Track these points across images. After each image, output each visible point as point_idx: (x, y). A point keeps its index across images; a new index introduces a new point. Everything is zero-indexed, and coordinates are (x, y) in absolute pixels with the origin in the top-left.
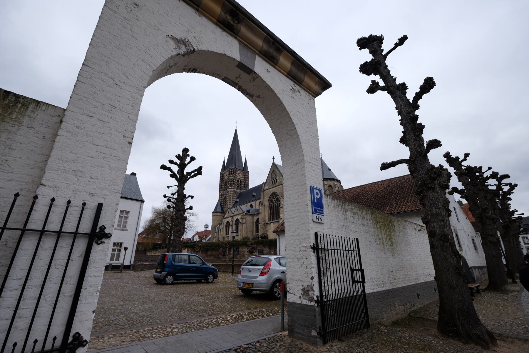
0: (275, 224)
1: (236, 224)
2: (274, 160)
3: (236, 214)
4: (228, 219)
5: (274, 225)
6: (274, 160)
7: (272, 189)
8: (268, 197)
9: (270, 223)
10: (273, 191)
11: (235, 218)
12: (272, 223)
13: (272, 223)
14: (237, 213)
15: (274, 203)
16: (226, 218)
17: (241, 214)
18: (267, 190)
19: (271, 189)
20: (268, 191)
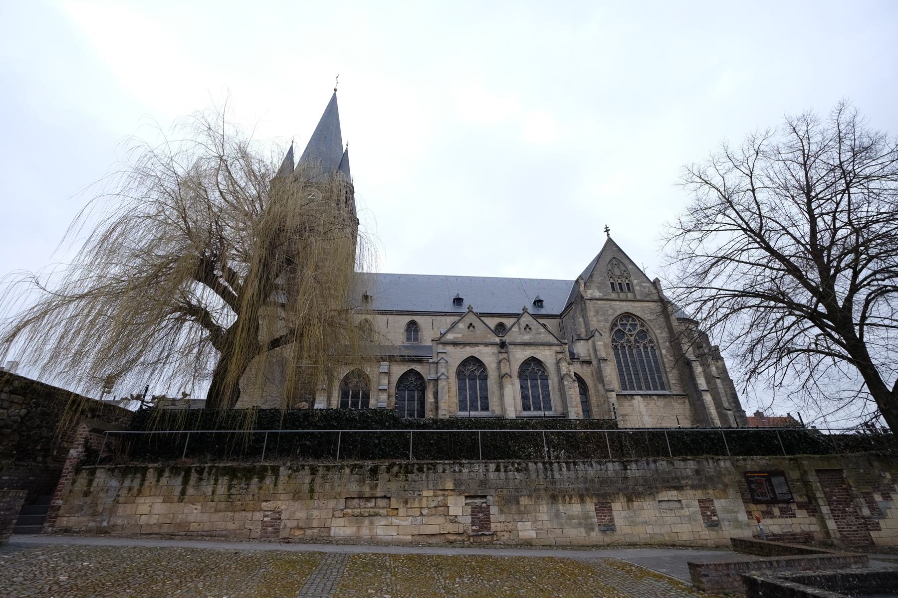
0: (652, 403)
1: (522, 375)
2: (608, 235)
3: (519, 340)
4: (468, 348)
5: (648, 404)
6: (608, 235)
7: (617, 303)
8: (606, 321)
9: (632, 395)
10: (625, 310)
11: (520, 355)
12: (638, 399)
13: (638, 399)
14: (526, 338)
15: (628, 341)
16: (455, 344)
17: (550, 345)
18: (599, 302)
19: (613, 303)
20: (603, 304)
